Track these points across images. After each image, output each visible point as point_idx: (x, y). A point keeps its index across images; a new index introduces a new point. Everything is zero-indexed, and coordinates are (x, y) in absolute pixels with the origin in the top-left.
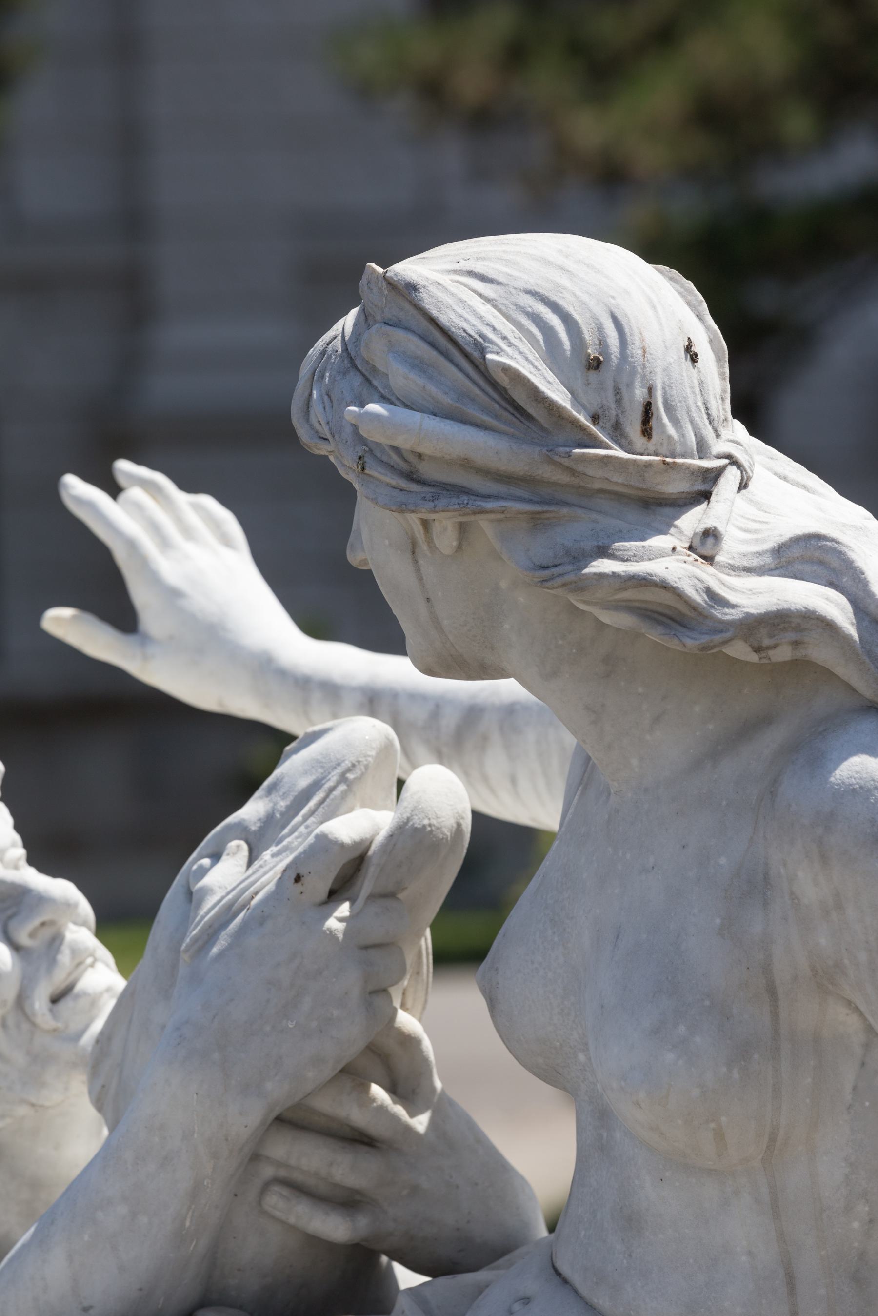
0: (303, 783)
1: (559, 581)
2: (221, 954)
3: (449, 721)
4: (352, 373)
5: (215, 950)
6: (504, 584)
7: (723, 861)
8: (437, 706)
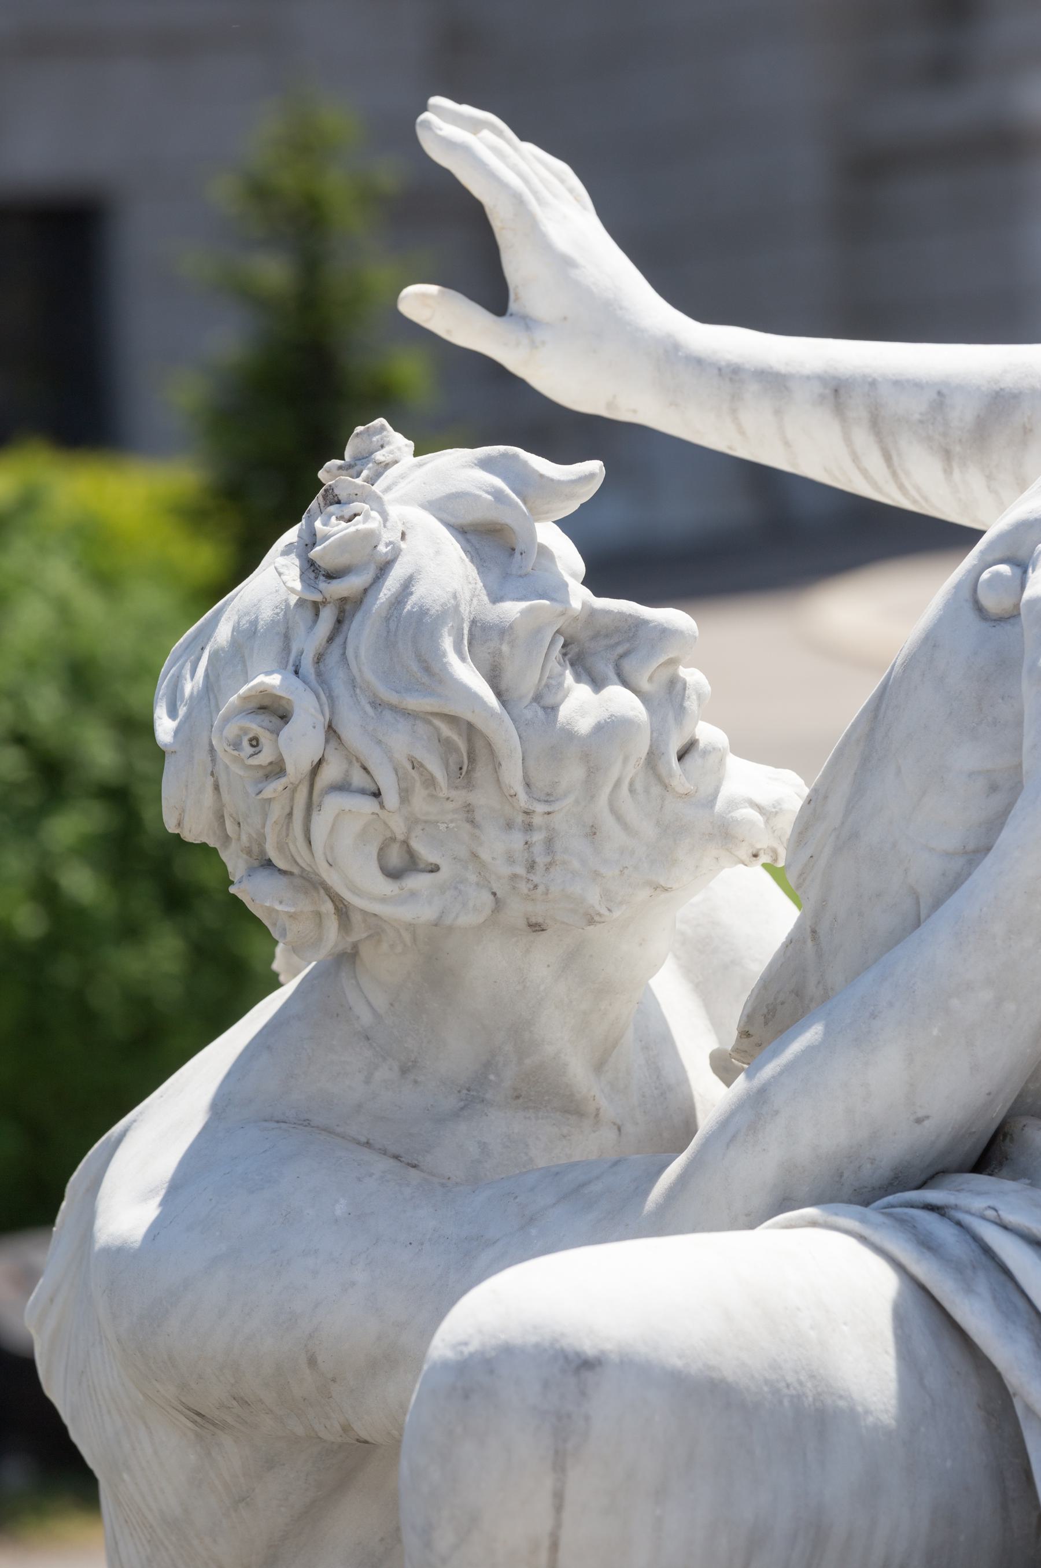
3: (963, 413)
8: (939, 393)
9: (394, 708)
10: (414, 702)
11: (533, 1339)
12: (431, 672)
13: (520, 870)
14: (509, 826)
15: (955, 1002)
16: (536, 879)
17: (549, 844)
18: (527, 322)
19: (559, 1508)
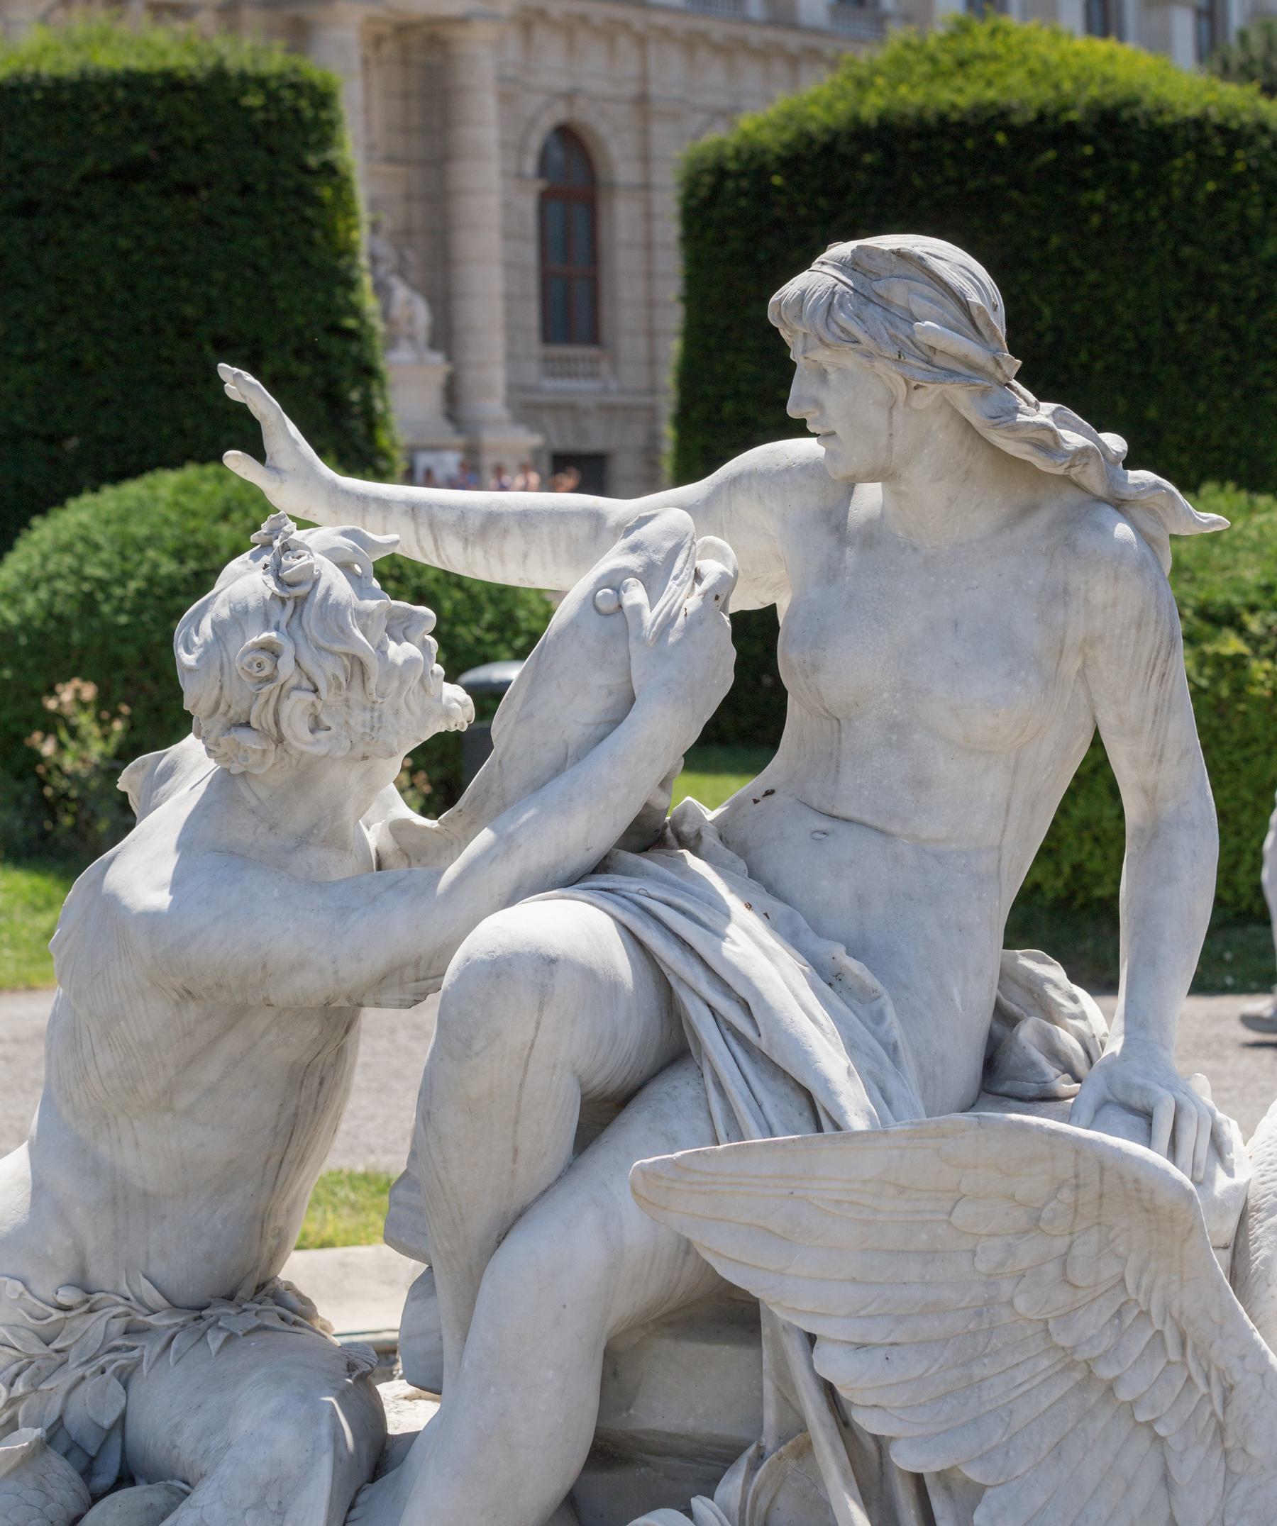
0: (669, 544)
1: (1005, 425)
2: (679, 643)
3: (474, 522)
4: (871, 305)
5: (671, 639)
6: (934, 428)
7: (1031, 582)
9: (326, 650)
10: (337, 647)
11: (528, 949)
12: (344, 632)
13: (368, 731)
14: (365, 709)
15: (611, 794)
16: (374, 734)
17: (380, 717)
18: (276, 470)
19: (537, 1029)
